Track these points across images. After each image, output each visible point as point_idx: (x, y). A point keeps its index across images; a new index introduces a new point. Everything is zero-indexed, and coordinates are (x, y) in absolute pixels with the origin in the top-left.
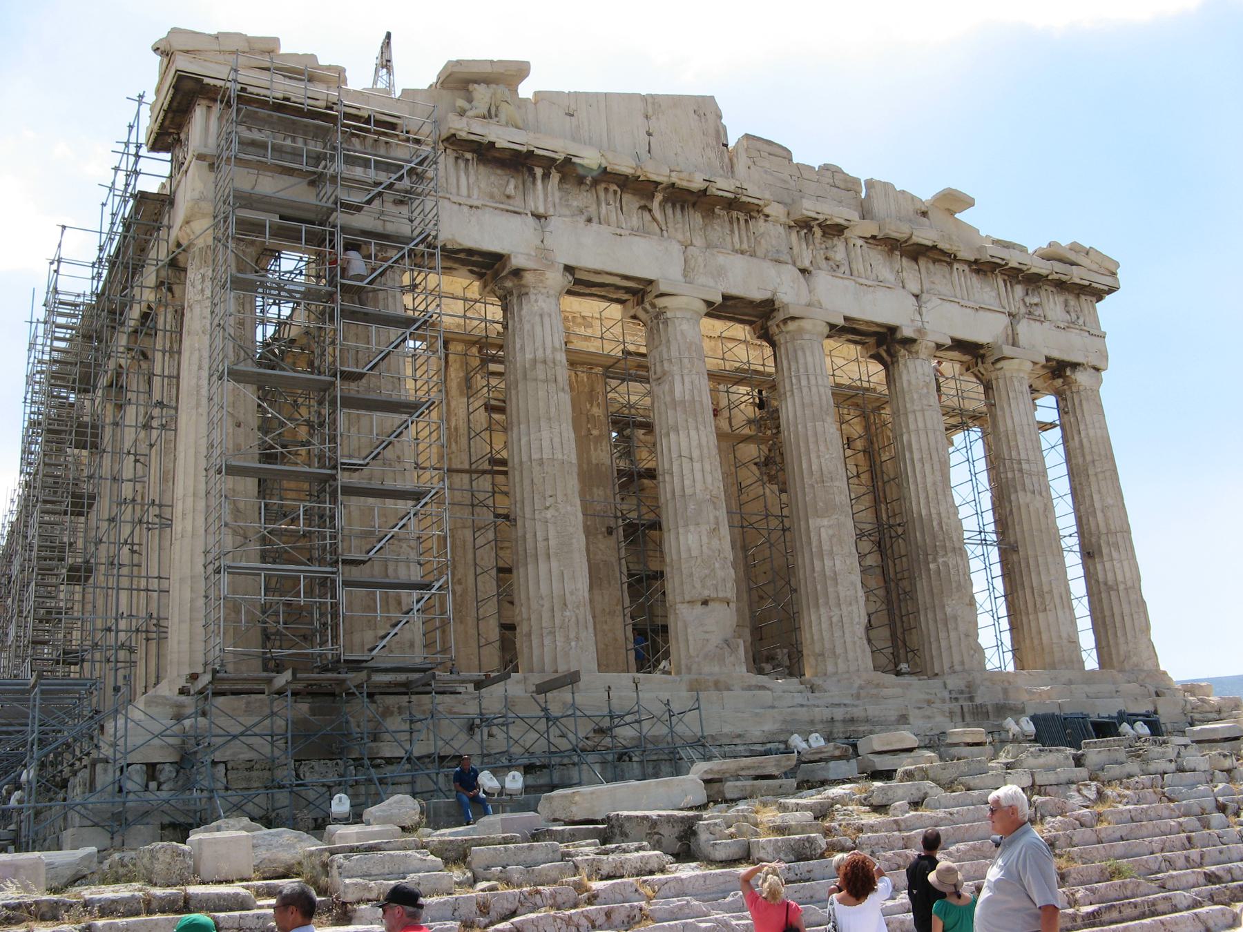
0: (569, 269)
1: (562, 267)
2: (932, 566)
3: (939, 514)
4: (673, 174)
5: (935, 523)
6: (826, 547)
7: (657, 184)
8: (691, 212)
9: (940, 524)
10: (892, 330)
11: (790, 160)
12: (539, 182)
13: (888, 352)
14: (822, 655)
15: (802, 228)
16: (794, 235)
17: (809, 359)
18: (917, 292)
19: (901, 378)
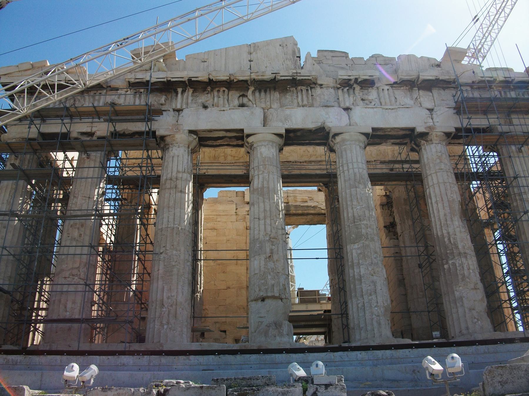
0: (191, 132)
1: (187, 132)
2: (446, 266)
3: (448, 233)
4: (252, 74)
5: (446, 239)
6: (355, 261)
7: (246, 81)
8: (272, 92)
9: (449, 239)
10: (413, 130)
11: (348, 57)
12: (179, 95)
13: (415, 144)
14: (354, 328)
15: (345, 87)
16: (340, 91)
17: (349, 155)
18: (430, 107)
19: (423, 156)
